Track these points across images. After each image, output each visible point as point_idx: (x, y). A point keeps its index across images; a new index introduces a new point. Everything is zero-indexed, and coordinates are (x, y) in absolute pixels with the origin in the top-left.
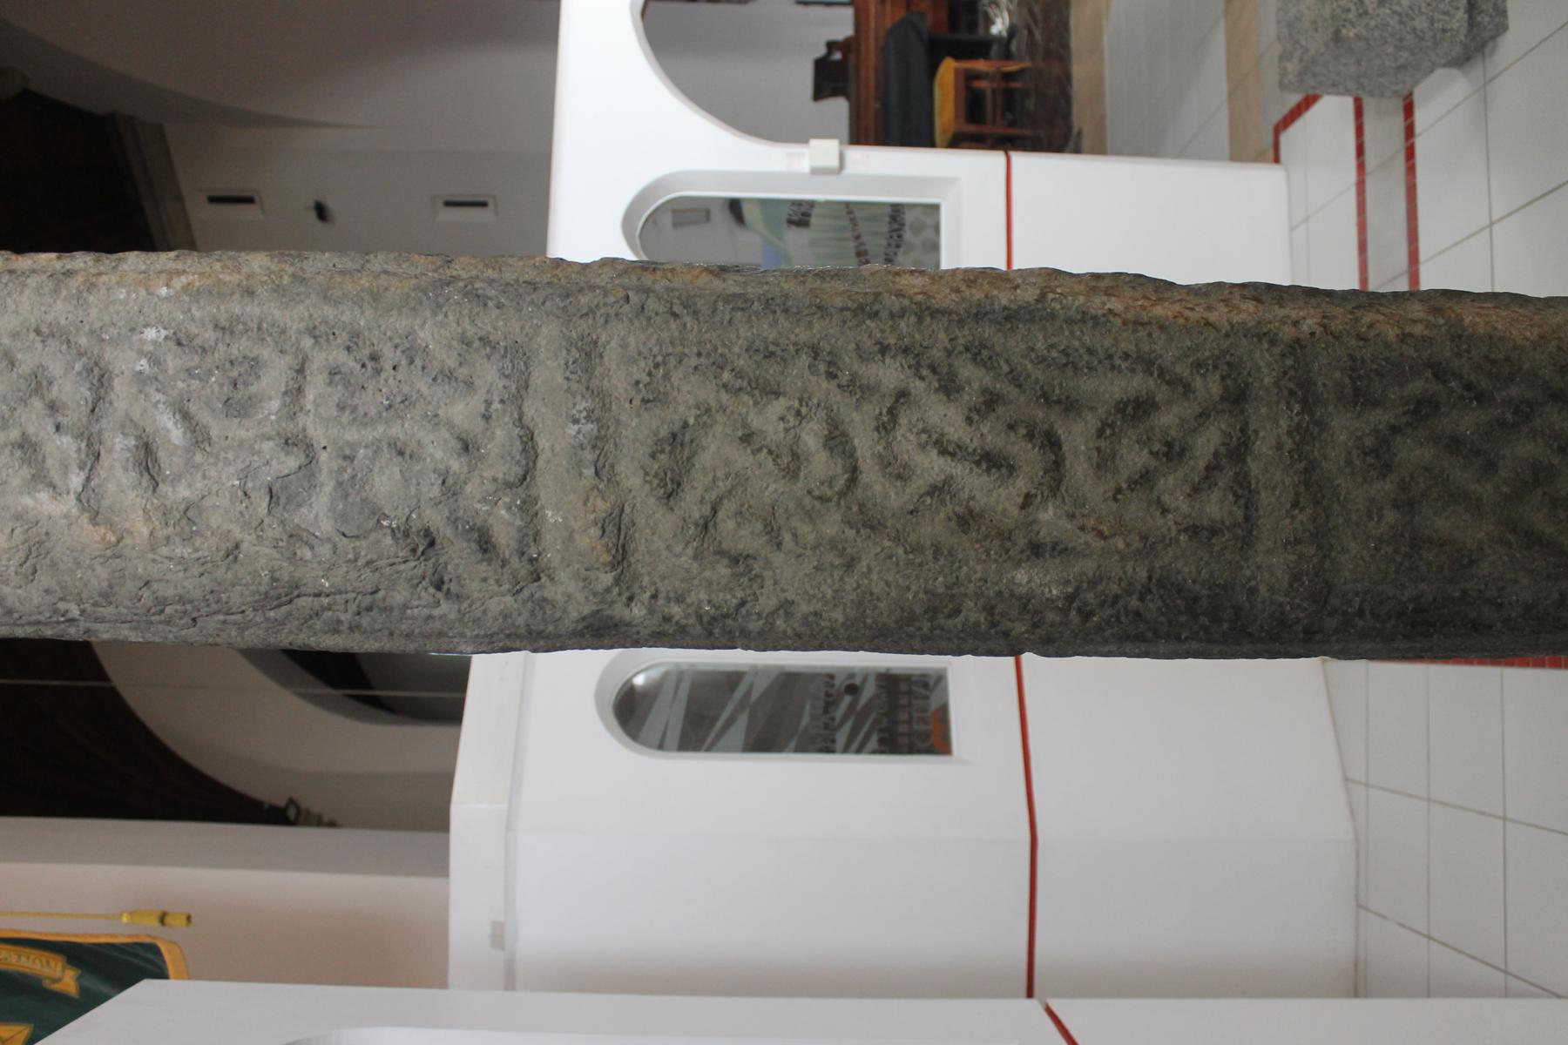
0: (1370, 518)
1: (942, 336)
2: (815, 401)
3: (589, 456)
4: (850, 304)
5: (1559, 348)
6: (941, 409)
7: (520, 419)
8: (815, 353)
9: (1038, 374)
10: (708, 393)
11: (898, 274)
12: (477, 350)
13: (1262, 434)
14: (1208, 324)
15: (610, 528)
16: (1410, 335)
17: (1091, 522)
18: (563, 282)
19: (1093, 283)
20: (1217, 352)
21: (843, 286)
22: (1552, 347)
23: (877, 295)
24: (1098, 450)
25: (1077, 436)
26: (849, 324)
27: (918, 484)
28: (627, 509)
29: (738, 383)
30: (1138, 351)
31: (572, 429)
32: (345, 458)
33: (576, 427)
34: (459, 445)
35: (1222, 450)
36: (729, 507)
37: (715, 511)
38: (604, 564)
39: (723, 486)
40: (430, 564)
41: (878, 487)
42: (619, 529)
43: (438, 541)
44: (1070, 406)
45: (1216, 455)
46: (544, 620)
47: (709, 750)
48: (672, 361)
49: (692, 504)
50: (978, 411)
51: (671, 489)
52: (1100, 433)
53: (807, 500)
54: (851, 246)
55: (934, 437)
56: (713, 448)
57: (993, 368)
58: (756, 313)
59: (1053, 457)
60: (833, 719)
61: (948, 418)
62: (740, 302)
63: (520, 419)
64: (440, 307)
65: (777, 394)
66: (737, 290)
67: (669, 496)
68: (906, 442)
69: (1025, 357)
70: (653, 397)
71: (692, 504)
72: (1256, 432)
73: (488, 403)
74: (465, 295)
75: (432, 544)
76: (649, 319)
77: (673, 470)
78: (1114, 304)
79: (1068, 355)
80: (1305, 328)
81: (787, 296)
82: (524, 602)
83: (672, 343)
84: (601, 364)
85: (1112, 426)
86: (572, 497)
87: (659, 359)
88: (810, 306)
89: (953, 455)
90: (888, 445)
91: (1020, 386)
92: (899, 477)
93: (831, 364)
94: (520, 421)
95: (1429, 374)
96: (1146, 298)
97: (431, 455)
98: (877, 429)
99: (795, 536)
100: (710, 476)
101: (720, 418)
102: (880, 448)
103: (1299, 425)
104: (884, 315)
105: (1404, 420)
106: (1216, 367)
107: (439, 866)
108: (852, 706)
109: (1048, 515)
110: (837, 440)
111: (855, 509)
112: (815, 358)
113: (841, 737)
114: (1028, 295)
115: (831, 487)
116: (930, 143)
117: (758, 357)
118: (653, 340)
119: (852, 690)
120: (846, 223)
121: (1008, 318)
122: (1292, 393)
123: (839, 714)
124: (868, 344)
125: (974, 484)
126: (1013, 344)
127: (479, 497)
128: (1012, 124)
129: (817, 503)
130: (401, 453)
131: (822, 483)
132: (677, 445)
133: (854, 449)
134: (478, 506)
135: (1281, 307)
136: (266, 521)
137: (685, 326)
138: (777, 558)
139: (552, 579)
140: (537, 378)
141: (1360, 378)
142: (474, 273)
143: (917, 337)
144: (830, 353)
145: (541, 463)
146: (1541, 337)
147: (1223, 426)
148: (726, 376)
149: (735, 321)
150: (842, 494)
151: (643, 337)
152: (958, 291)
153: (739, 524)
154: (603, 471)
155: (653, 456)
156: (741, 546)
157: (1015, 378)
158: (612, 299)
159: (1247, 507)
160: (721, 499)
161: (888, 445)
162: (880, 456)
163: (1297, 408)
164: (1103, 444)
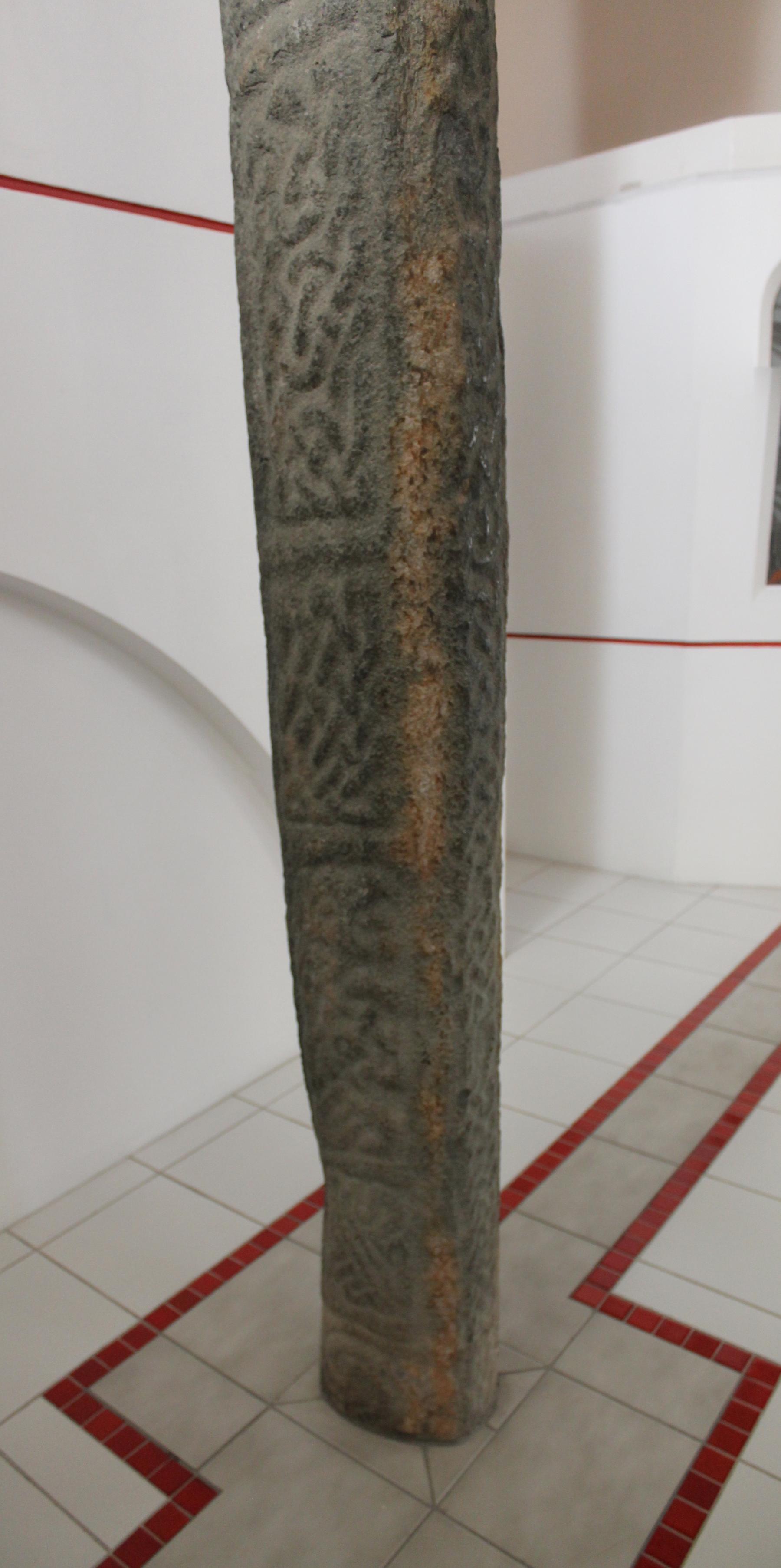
0: (293, 600)
1: (375, 291)
2: (324, 204)
5: (399, 745)
8: (356, 196)
10: (325, 120)
13: (330, 528)
14: (395, 492)
15: (254, 76)
16: (400, 641)
17: (279, 413)
22: (399, 740)
24: (311, 413)
25: (319, 398)
29: (330, 142)
30: (372, 439)
31: (296, 25)
35: (316, 499)
42: (256, 84)
44: (335, 391)
45: (313, 495)
49: (273, 130)
50: (325, 324)
52: (319, 413)
55: (310, 295)
57: (353, 331)
58: (380, 146)
59: (307, 381)
61: (322, 305)
65: (329, 174)
68: (309, 275)
69: (362, 357)
72: (330, 524)
76: (370, 58)
78: (410, 424)
80: (400, 565)
83: (355, 82)
84: (339, 30)
85: (323, 421)
87: (341, 75)
90: (304, 263)
91: (342, 352)
93: (347, 210)
95: (369, 647)
96: (424, 451)
102: (303, 258)
104: (387, 245)
105: (339, 625)
106: (362, 494)
109: (281, 384)
110: (310, 224)
111: (276, 249)
112: (349, 196)
121: (389, 341)
122: (349, 548)
126: (373, 346)
135: (425, 554)
137: (369, 89)
138: (252, 204)
141: (362, 597)
146: (408, 735)
147: (330, 500)
148: (335, 131)
155: (287, 92)
157: (348, 349)
159: (293, 518)
163: (341, 551)
164: (314, 415)
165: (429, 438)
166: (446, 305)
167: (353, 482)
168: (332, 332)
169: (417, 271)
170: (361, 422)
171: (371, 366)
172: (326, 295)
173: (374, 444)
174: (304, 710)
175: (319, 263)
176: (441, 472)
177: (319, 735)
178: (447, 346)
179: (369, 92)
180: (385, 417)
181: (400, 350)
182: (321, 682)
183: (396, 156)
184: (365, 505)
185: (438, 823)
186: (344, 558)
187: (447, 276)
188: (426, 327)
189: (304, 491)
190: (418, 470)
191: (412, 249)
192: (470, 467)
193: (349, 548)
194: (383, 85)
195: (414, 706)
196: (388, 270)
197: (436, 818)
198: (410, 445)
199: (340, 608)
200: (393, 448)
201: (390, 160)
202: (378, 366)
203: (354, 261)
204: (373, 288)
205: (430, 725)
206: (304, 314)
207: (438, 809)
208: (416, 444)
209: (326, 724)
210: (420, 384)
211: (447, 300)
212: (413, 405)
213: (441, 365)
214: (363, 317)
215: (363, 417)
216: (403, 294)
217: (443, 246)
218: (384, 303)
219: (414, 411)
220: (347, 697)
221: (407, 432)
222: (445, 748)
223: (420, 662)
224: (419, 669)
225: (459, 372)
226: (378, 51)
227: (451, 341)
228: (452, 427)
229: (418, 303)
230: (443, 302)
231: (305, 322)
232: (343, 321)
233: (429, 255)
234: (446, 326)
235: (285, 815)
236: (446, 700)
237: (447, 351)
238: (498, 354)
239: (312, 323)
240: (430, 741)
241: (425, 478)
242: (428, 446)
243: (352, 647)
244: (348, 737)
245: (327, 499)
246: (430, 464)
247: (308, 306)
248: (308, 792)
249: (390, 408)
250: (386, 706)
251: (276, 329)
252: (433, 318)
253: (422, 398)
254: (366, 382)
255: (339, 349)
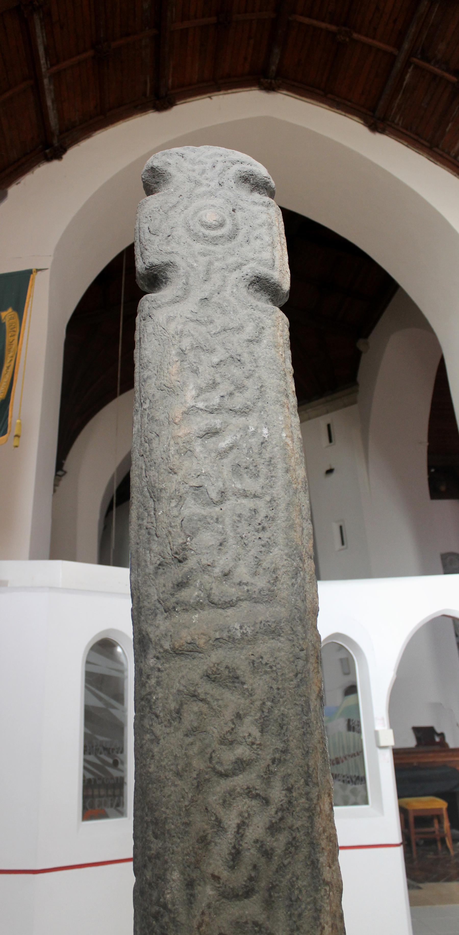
2: (260, 752)
3: (225, 635)
4: (311, 769)
6: (261, 824)
7: (240, 600)
9: (285, 882)
10: (260, 694)
11: (329, 795)
12: (271, 576)
15: (191, 647)
18: (307, 617)
19: (338, 915)
21: (320, 764)
23: (317, 784)
26: (301, 769)
27: (221, 812)
28: (201, 655)
29: (266, 711)
31: (237, 626)
32: (217, 519)
33: (238, 628)
34: (226, 571)
36: (204, 708)
37: (202, 700)
38: (174, 645)
39: (214, 704)
40: (171, 561)
41: (218, 789)
42: (190, 651)
43: (181, 564)
44: (269, 904)
46: (147, 615)
47: (86, 687)
48: (274, 675)
49: (205, 688)
50: (262, 846)
51: (211, 677)
53: (209, 750)
54: (340, 755)
55: (247, 821)
56: (233, 698)
58: (301, 718)
59: (240, 893)
60: (101, 753)
61: (256, 830)
62: (306, 710)
63: (240, 600)
64: (290, 557)
66: (312, 707)
67: (207, 676)
68: (243, 804)
69: (293, 874)
70: (256, 665)
71: (205, 688)
73: (246, 584)
74: (296, 568)
75: (180, 561)
76: (294, 662)
77: (221, 678)
79: (296, 901)
81: (312, 734)
82: (154, 605)
83: (283, 674)
84: (269, 639)
86: (205, 627)
87: (274, 668)
88: (308, 747)
89: (238, 832)
90: (240, 794)
91: (277, 871)
92: (224, 801)
93: (280, 760)
94: (239, 600)
97: (221, 559)
98: (248, 788)
99: (192, 744)
100: (218, 697)
101: (248, 701)
102: (239, 789)
104: (307, 789)
107: (34, 556)
108: (107, 764)
111: (207, 777)
113: (92, 758)
114: (327, 875)
115: (217, 763)
116: (400, 796)
117: (279, 721)
118: (283, 665)
119: (116, 764)
120: (352, 752)
121: (313, 863)
123: (103, 756)
124: (291, 781)
125: (223, 846)
127: (203, 581)
128: (417, 845)
129: (208, 756)
130: (221, 544)
131: (219, 758)
132: (234, 680)
133: (237, 775)
134: (198, 581)
136: (187, 485)
137: (292, 681)
139: (166, 618)
140: (260, 607)
142: (307, 570)
143: (298, 809)
144: (285, 760)
145: (220, 611)
149: (297, 707)
150: (214, 769)
151: (284, 659)
152: (324, 831)
153: (196, 713)
154: (218, 643)
156: (185, 715)
157: (281, 868)
158: (301, 642)
160: (208, 703)
161: (240, 794)
162: (234, 790)
164: (250, 925)
179: (292, 683)
180: (312, 927)
181: (319, 870)
183: (309, 726)
194: (301, 680)
196: (310, 807)
201: (307, 730)
202: (305, 883)
214: (294, 843)
218: (308, 832)
226: (298, 658)
231: (241, 843)
233: (325, 793)
247: (244, 830)
254: (298, 898)
255: (274, 867)
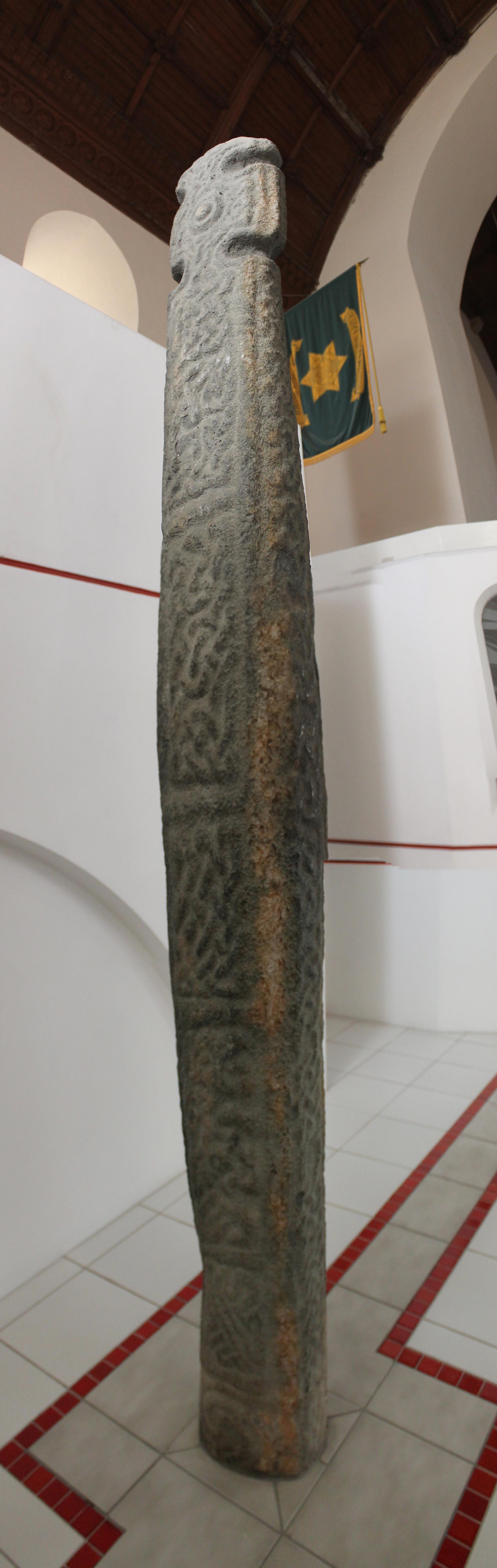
1: (240, 643)
5: (254, 940)
16: (254, 867)
20: (237, 770)
22: (254, 936)
30: (237, 731)
44: (214, 700)
61: (208, 649)
68: (200, 631)
78: (261, 723)
91: (219, 677)
96: (270, 741)
103: (209, 807)
104: (248, 617)
106: (228, 768)
121: (248, 672)
126: (238, 674)
146: (260, 933)
157: (223, 675)
163: (216, 806)
165: (273, 733)
166: (283, 652)
167: (223, 760)
168: (214, 665)
169: (265, 632)
170: (229, 721)
171: (236, 686)
172: (211, 643)
173: (238, 735)
174: (190, 917)
175: (207, 625)
176: (281, 755)
177: (201, 934)
178: (283, 675)
181: (255, 678)
182: (202, 897)
184: (231, 776)
185: (280, 994)
186: (218, 811)
187: (283, 635)
188: (271, 664)
189: (191, 764)
190: (266, 753)
191: (262, 619)
192: (299, 752)
193: (221, 804)
195: (264, 911)
197: (279, 991)
198: (260, 737)
199: (215, 846)
200: (249, 738)
203: (228, 625)
204: (240, 641)
205: (274, 925)
206: (197, 653)
207: (280, 984)
208: (264, 736)
209: (205, 926)
210: (267, 698)
211: (283, 649)
212: (262, 711)
213: (280, 687)
215: (231, 718)
216: (257, 645)
217: (280, 618)
219: (263, 715)
220: (219, 907)
221: (259, 728)
222: (285, 941)
223: (267, 881)
224: (267, 886)
225: (291, 691)
227: (286, 673)
228: (288, 726)
229: (266, 650)
230: (281, 650)
232: (220, 658)
234: (283, 664)
235: (177, 992)
236: (285, 907)
237: (284, 678)
238: (315, 680)
239: (201, 659)
240: (274, 936)
241: (270, 759)
242: (272, 737)
243: (222, 872)
244: (220, 935)
245: (205, 770)
246: (273, 750)
248: (193, 975)
249: (248, 713)
250: (245, 912)
251: (179, 661)
252: (275, 659)
253: (268, 706)
255: (217, 675)
